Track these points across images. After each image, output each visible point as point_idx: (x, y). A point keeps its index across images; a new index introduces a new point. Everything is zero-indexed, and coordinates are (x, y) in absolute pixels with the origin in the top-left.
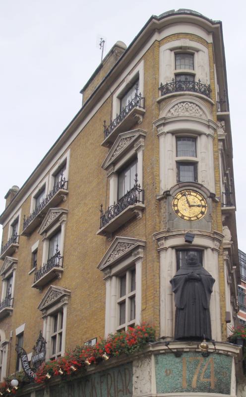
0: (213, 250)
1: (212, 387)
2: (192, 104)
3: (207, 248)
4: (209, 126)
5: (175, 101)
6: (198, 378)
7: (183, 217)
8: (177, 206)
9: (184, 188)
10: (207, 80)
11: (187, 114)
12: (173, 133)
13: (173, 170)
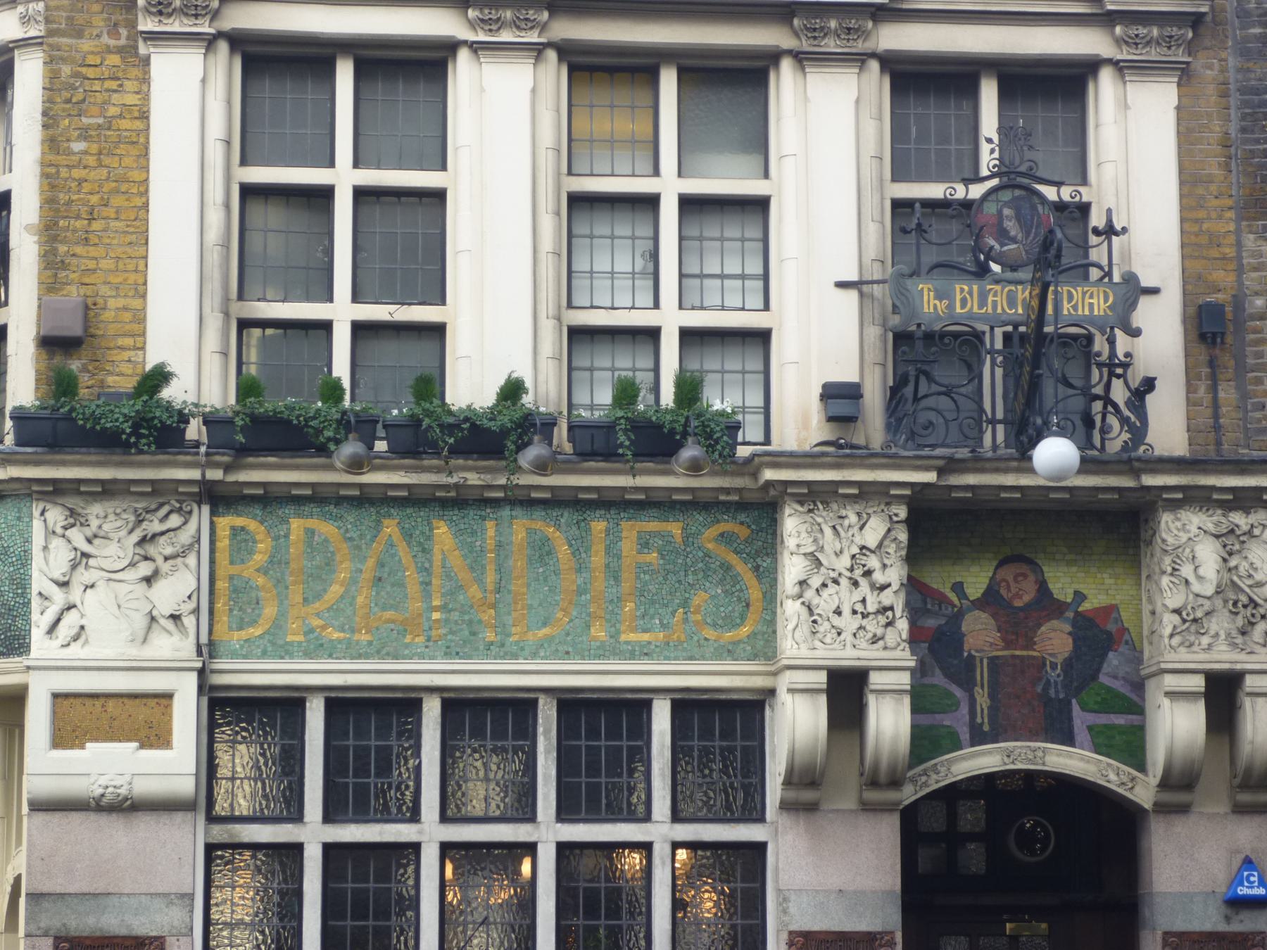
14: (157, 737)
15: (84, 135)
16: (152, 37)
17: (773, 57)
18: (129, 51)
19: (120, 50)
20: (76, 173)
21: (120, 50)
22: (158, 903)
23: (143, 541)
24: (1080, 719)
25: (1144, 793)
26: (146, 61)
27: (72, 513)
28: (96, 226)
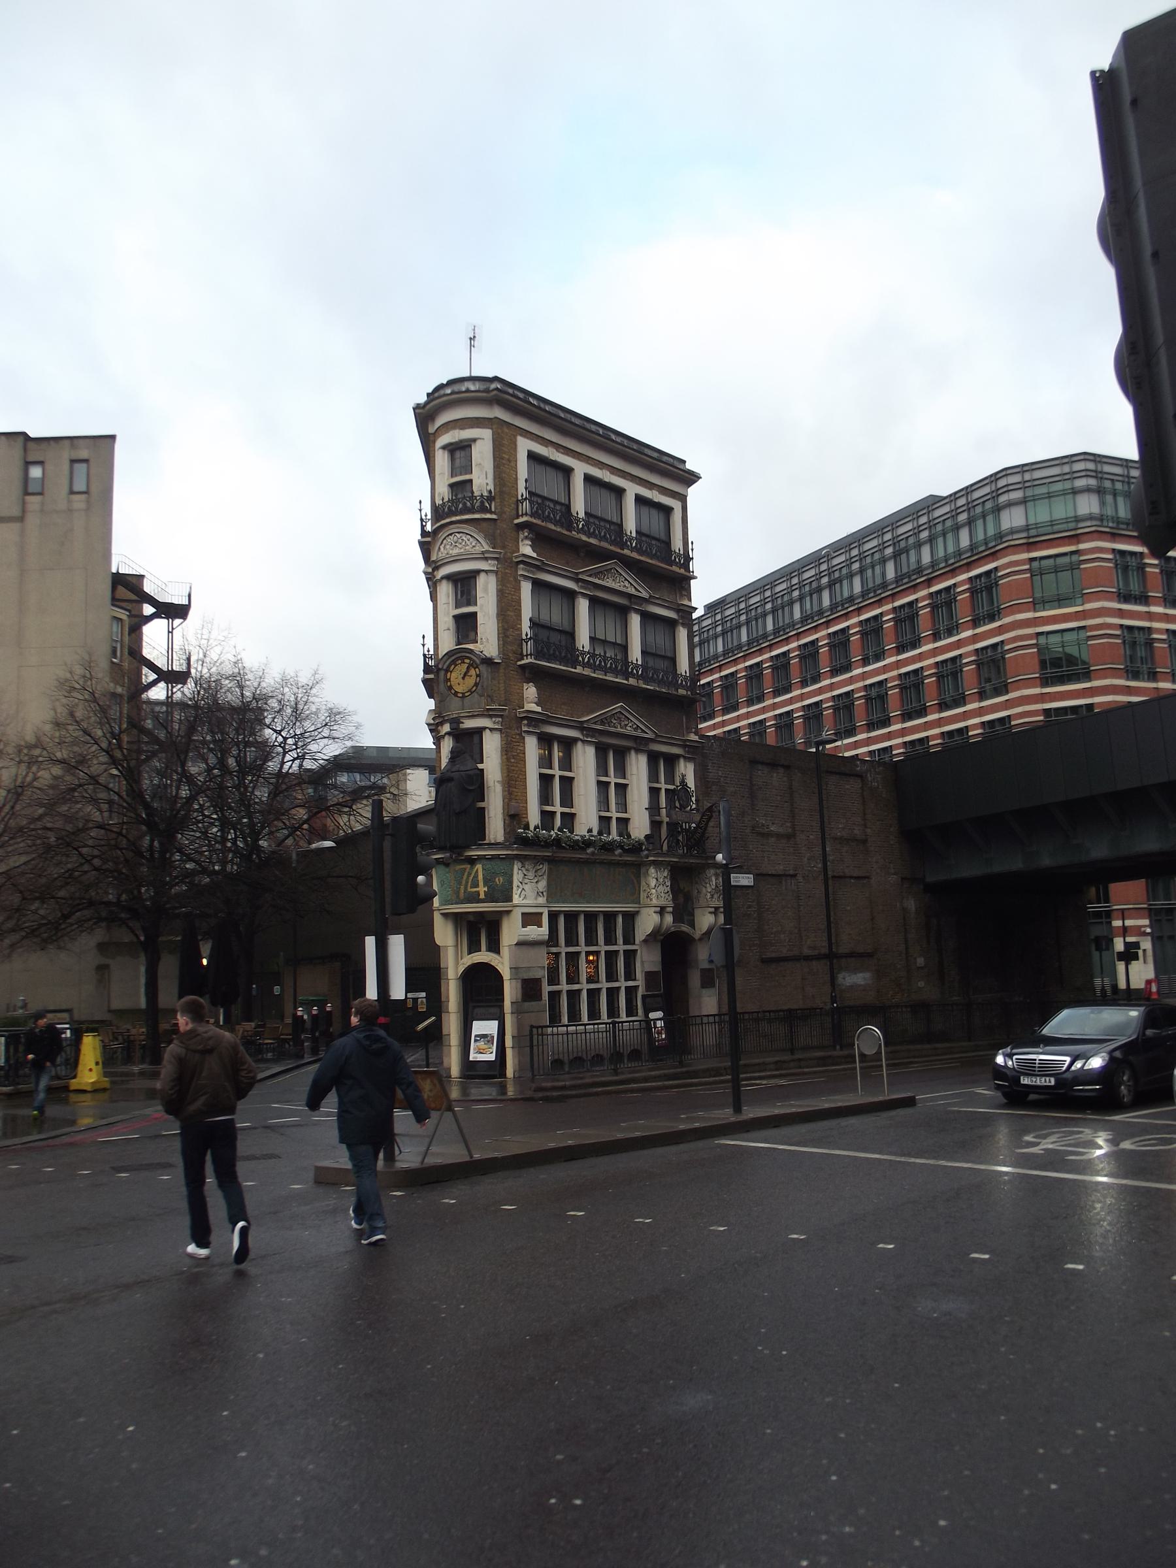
0: (491, 730)
1: (482, 896)
2: (461, 534)
3: (485, 728)
4: (486, 559)
5: (442, 535)
6: (466, 888)
7: (456, 693)
8: (449, 680)
9: (453, 658)
10: (487, 484)
11: (455, 551)
12: (448, 577)
13: (449, 629)
14: (540, 926)
15: (514, 757)
16: (525, 731)
17: (629, 749)
18: (520, 735)
19: (519, 734)
20: (513, 768)
21: (519, 734)
22: (539, 969)
23: (536, 871)
24: (686, 918)
25: (697, 935)
26: (524, 738)
27: (522, 863)
28: (517, 783)
